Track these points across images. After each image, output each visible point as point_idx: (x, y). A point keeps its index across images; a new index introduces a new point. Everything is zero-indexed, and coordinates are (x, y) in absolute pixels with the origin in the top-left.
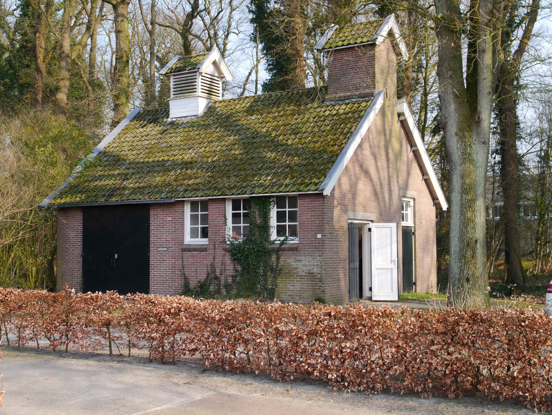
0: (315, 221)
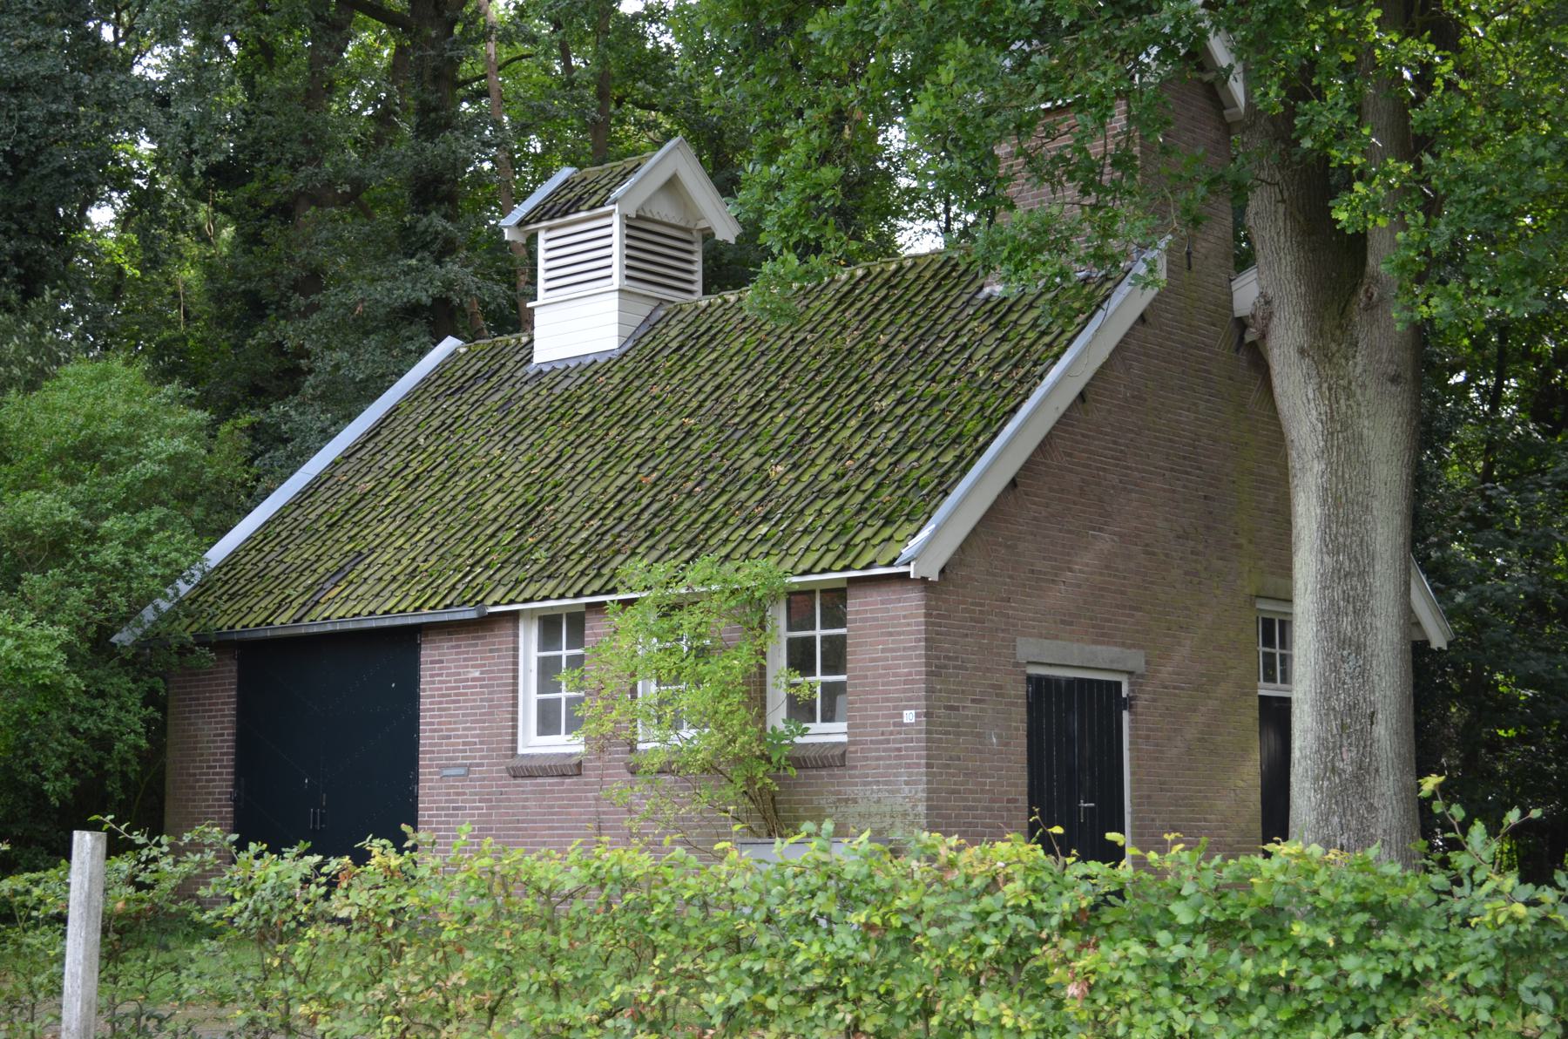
0: (898, 666)
